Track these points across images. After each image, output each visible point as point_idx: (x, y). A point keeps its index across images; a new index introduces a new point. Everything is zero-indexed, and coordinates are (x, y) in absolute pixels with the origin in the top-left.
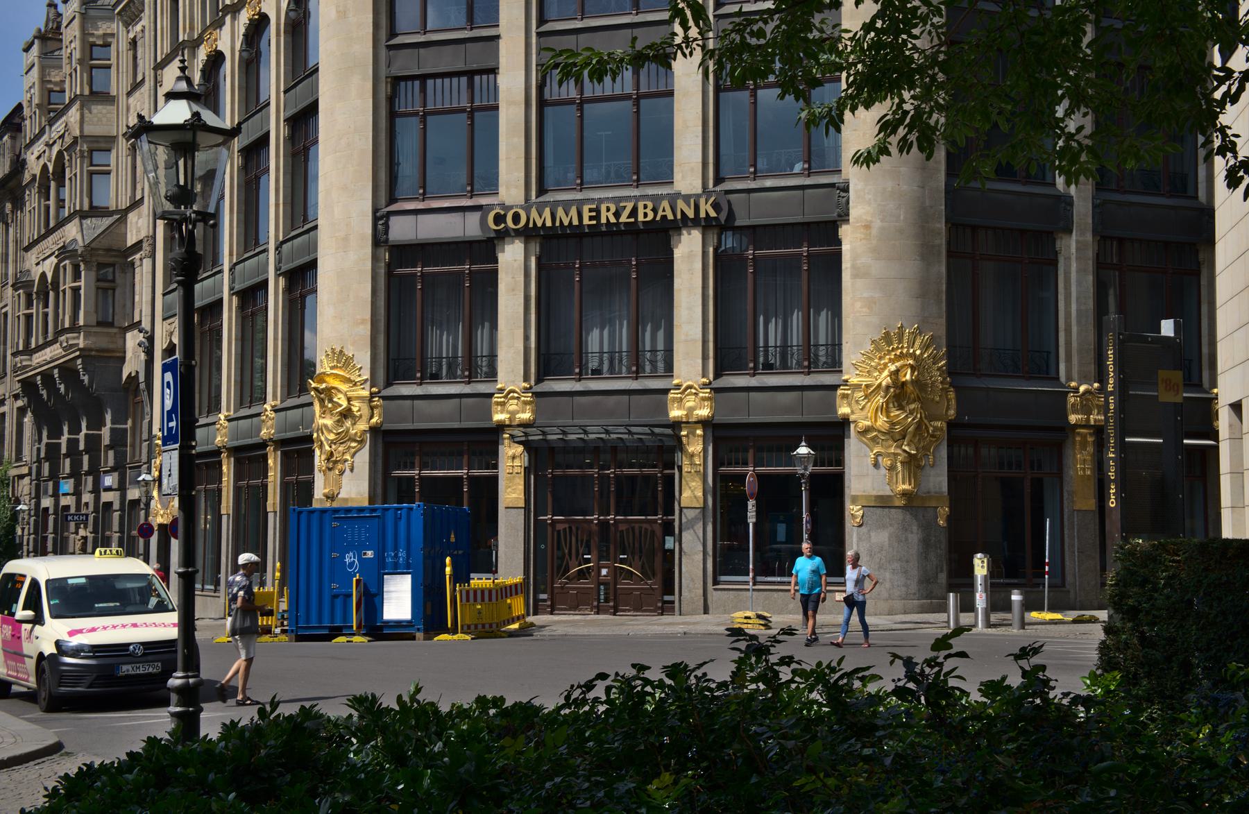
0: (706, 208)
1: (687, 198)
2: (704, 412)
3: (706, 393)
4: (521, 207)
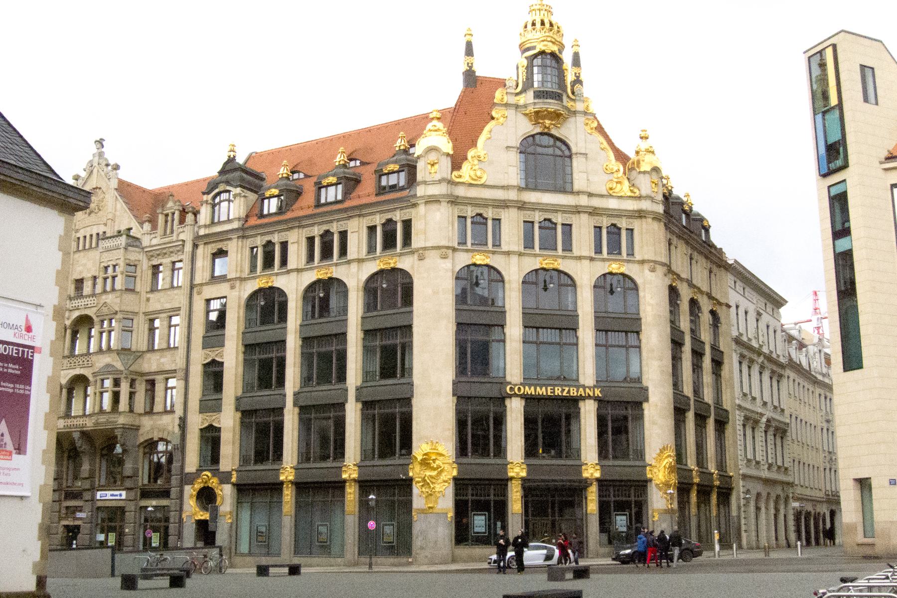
0: (598, 392)
1: (590, 388)
2: (597, 475)
3: (598, 467)
4: (521, 384)
